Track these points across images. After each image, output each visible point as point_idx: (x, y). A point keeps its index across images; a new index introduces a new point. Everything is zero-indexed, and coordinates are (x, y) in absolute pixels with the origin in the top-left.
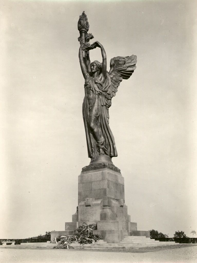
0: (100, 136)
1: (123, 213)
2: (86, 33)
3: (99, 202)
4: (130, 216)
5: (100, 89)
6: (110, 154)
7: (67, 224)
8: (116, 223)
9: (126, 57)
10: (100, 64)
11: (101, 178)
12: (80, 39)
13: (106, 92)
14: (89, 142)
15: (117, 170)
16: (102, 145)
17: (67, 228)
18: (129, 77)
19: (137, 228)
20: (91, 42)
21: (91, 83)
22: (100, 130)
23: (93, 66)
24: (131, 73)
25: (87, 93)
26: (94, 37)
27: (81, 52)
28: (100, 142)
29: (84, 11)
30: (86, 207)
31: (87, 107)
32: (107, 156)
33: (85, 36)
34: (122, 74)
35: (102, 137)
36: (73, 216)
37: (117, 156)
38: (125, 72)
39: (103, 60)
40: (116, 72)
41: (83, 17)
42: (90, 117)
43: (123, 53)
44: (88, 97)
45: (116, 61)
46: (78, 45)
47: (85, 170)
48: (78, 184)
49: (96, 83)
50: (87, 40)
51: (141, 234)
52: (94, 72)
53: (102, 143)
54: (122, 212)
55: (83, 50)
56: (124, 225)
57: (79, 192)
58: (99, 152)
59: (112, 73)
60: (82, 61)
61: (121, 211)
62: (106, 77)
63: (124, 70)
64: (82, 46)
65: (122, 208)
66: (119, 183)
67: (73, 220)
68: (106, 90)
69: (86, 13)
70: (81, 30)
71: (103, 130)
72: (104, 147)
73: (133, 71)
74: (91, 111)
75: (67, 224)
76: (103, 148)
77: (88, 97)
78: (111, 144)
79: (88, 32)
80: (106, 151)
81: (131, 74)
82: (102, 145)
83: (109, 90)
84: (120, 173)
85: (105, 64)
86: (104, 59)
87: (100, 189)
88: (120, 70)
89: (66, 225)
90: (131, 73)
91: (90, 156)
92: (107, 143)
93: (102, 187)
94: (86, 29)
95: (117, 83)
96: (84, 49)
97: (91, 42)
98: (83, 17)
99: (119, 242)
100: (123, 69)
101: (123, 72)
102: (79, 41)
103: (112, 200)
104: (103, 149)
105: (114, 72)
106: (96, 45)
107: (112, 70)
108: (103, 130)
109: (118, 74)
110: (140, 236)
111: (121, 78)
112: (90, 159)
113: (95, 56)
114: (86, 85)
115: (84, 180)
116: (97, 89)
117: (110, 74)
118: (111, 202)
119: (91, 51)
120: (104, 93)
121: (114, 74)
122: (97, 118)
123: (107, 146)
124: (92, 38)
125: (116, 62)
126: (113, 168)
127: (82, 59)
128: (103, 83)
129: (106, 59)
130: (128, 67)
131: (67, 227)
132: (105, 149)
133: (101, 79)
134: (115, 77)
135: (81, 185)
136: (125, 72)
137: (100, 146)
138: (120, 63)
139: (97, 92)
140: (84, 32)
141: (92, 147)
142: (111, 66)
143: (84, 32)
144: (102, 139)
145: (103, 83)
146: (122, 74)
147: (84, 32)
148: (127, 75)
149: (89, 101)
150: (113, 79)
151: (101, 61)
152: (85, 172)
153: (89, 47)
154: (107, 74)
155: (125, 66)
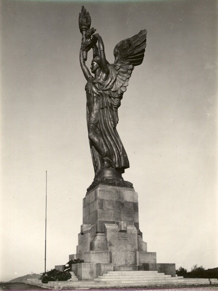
1: (127, 240)
4: (146, 243)
5: (99, 89)
8: (103, 254)
9: (132, 37)
13: (109, 90)
15: (129, 186)
18: (142, 60)
19: (155, 260)
22: (102, 140)
24: (142, 54)
28: (103, 154)
29: (83, 7)
34: (130, 60)
37: (129, 167)
38: (133, 57)
40: (122, 61)
45: (119, 47)
51: (150, 268)
53: (105, 155)
54: (126, 239)
55: (84, 51)
56: (129, 255)
59: (117, 64)
61: (121, 238)
63: (131, 54)
65: (122, 233)
66: (126, 202)
68: (108, 87)
70: (81, 28)
71: (104, 137)
72: (109, 159)
73: (144, 51)
76: (107, 159)
80: (111, 162)
81: (143, 55)
82: (106, 156)
84: (133, 188)
88: (126, 56)
90: (142, 54)
92: (110, 153)
94: (85, 25)
96: (84, 49)
99: (93, 279)
100: (132, 53)
101: (130, 57)
103: (106, 225)
104: (107, 161)
105: (119, 62)
108: (104, 137)
109: (125, 62)
110: (149, 271)
111: (131, 66)
117: (114, 66)
118: (105, 227)
120: (107, 92)
121: (120, 65)
126: (115, 183)
130: (135, 49)
132: (109, 161)
134: (122, 68)
136: (133, 57)
138: (124, 48)
140: (84, 30)
143: (84, 29)
146: (130, 60)
147: (84, 29)
150: (119, 71)
153: (89, 44)
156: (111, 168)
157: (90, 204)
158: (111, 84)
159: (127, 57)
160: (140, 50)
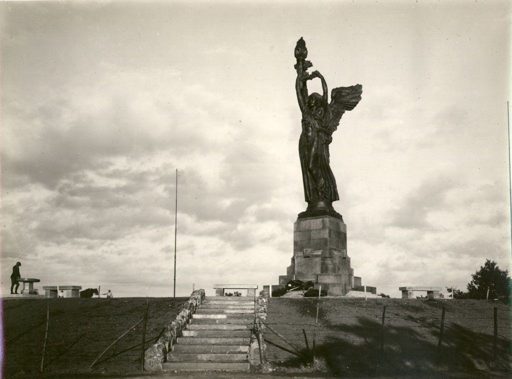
0: (320, 178)
2: (304, 60)
3: (319, 253)
6: (331, 198)
7: (281, 277)
10: (320, 97)
11: (321, 226)
12: (296, 67)
14: (306, 184)
15: (339, 217)
16: (322, 187)
17: (281, 283)
19: (361, 283)
20: (310, 71)
21: (309, 119)
23: (312, 99)
25: (305, 130)
26: (313, 64)
27: (298, 83)
29: (302, 37)
30: (304, 259)
31: (305, 146)
32: (328, 201)
33: (303, 64)
35: (322, 179)
36: (288, 268)
39: (324, 93)
41: (301, 44)
42: (309, 157)
43: (346, 82)
44: (306, 134)
46: (294, 74)
47: (302, 216)
48: (294, 232)
49: (315, 119)
50: (305, 69)
52: (313, 106)
57: (294, 241)
58: (318, 195)
60: (299, 94)
62: (326, 110)
64: (300, 77)
65: (344, 260)
67: (288, 273)
68: (326, 125)
69: (304, 39)
73: (357, 103)
74: (310, 150)
75: (281, 277)
77: (306, 134)
78: (332, 186)
79: (306, 59)
81: (355, 106)
83: (330, 124)
85: (326, 97)
86: (325, 92)
87: (320, 239)
89: (280, 279)
91: (307, 200)
93: (322, 237)
95: (338, 116)
97: (310, 71)
98: (301, 44)
101: (346, 103)
102: (296, 68)
103: (333, 251)
104: (322, 192)
106: (316, 74)
107: (333, 102)
112: (307, 204)
113: (314, 87)
114: (303, 121)
115: (301, 227)
116: (317, 126)
119: (308, 82)
120: (324, 129)
122: (316, 157)
123: (327, 190)
124: (310, 65)
125: (338, 92)
127: (299, 91)
128: (323, 117)
129: (327, 92)
131: (282, 281)
133: (321, 114)
135: (298, 233)
137: (319, 189)
139: (317, 128)
141: (309, 190)
142: (332, 97)
144: (322, 181)
145: (323, 117)
148: (351, 107)
149: (307, 139)
151: (322, 94)
152: (301, 219)
154: (328, 107)
155: (348, 97)
156: (325, 199)
157: (311, 230)
158: (328, 123)
159: (345, 102)
160: (354, 101)
